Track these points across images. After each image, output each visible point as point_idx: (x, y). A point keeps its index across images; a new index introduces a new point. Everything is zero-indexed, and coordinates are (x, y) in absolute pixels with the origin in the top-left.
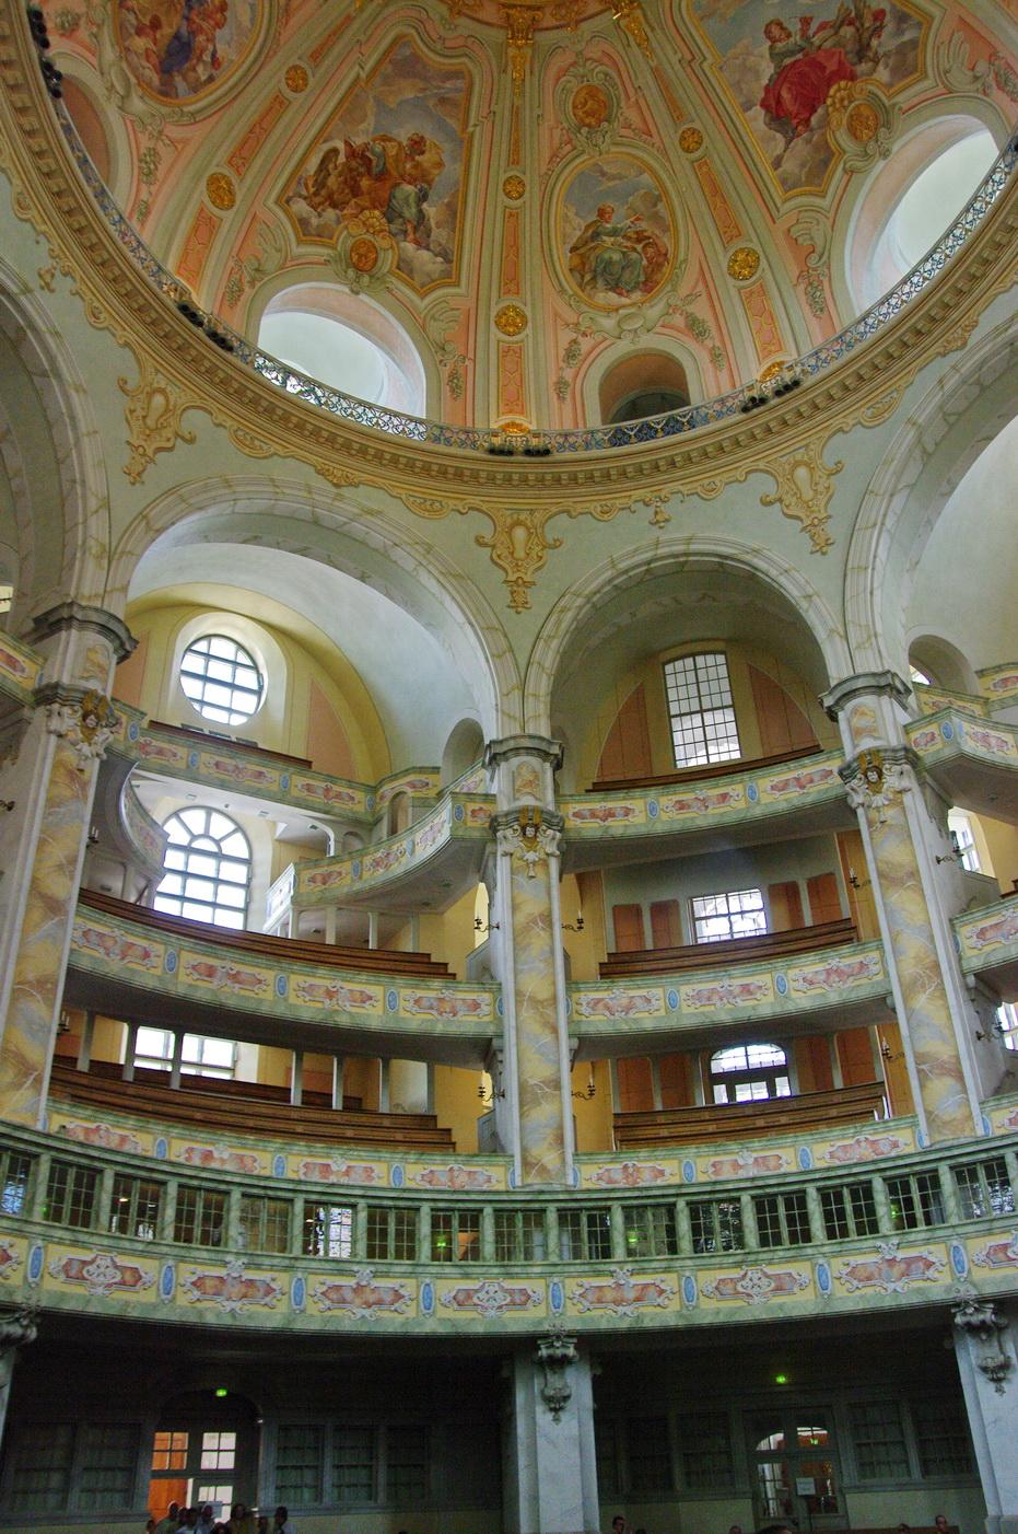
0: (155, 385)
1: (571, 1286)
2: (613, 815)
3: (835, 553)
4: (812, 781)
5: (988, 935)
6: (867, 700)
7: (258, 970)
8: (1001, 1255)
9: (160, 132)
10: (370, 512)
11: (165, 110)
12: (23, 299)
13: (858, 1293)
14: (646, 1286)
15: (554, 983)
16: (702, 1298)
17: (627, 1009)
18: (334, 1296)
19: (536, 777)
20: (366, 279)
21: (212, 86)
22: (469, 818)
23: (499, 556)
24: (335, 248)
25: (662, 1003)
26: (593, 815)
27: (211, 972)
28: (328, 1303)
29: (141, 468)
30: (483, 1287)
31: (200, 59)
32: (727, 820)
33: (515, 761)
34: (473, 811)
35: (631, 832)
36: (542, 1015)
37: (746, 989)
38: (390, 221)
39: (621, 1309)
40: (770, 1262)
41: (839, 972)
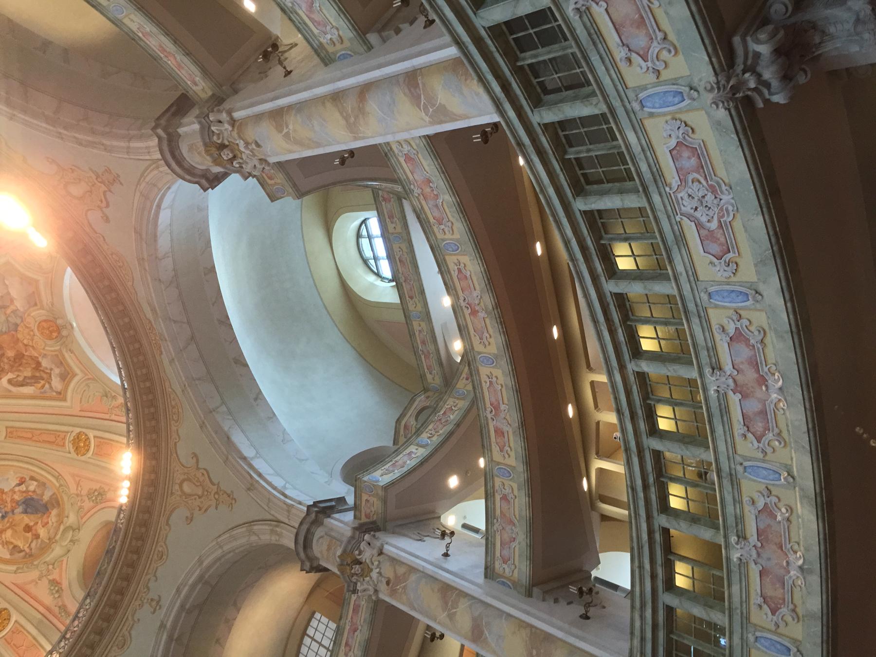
0: (179, 493)
1: (636, 74)
7: (484, 384)
9: (77, 495)
10: (153, 310)
11: (65, 499)
12: (169, 625)
18: (759, 426)
20: (59, 322)
21: (38, 477)
23: (102, 201)
24: (60, 351)
27: (499, 432)
28: (770, 436)
29: (225, 495)
30: (689, 217)
31: (27, 491)
36: (356, 117)
38: (17, 325)
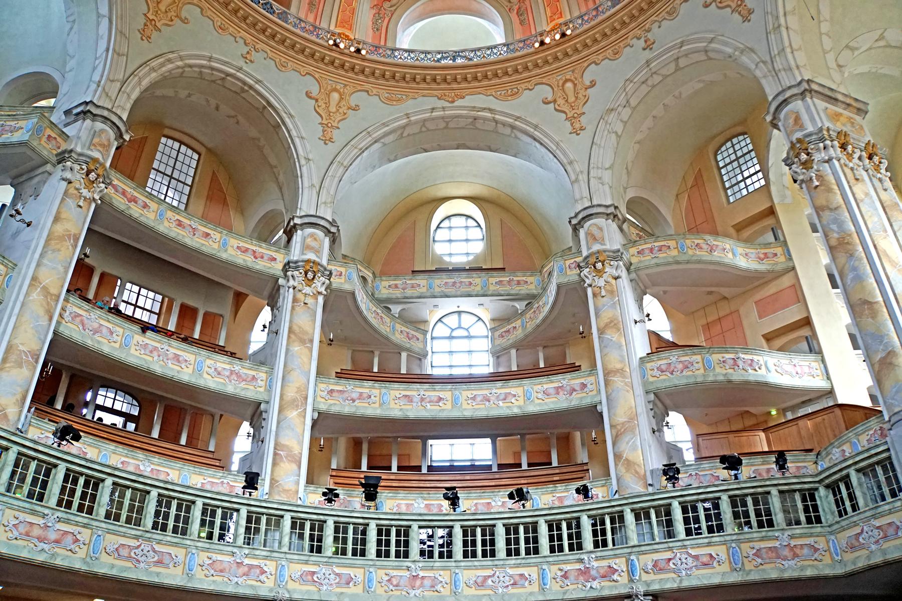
2: (136, 202)
3: (332, 148)
4: (262, 257)
5: (334, 394)
6: (320, 234)
8: (309, 577)
13: (211, 578)
14: (66, 533)
15: (62, 286)
16: (104, 553)
17: (96, 332)
19: (109, 145)
22: (44, 139)
25: (119, 339)
26: (124, 193)
32: (204, 249)
33: (99, 125)
34: (49, 136)
35: (143, 219)
37: (177, 358)
39: (42, 545)
40: (159, 542)
41: (238, 375)
